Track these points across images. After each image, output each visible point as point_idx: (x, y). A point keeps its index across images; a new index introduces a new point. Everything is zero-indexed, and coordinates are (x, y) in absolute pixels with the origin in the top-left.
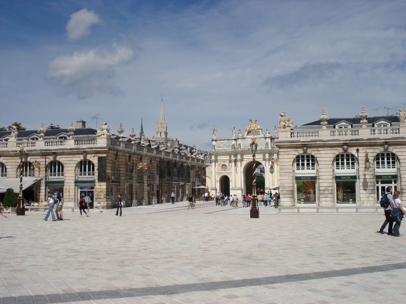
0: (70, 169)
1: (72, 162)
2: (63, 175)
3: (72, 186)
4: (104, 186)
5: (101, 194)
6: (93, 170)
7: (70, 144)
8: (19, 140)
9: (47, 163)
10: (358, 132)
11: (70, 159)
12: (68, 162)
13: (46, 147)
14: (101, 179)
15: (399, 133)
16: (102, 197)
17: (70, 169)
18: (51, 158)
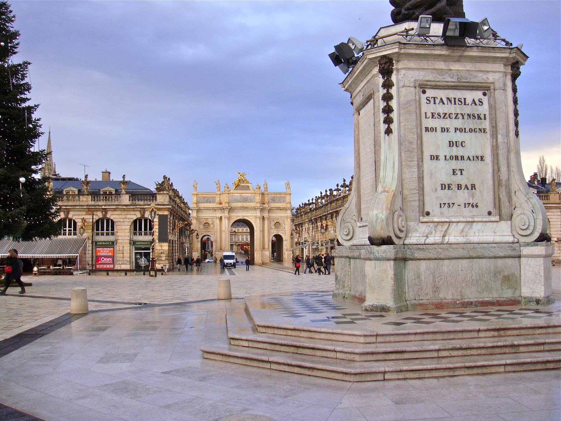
0: (124, 227)
1: (126, 220)
2: (113, 234)
3: (127, 247)
4: (165, 246)
5: (162, 255)
6: (151, 228)
9: (95, 220)
11: (124, 217)
12: (122, 220)
14: (163, 238)
16: (164, 258)
17: (124, 227)
18: (100, 215)
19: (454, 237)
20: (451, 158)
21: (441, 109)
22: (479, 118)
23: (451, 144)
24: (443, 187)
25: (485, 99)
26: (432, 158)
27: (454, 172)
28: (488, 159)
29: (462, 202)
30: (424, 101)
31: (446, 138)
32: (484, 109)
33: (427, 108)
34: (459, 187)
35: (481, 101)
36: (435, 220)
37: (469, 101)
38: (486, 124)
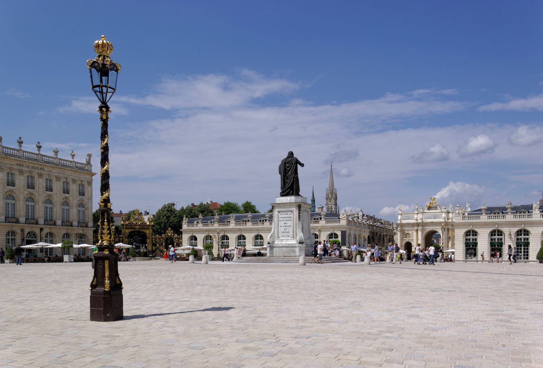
7: (322, 223)
8: (237, 222)
10: (480, 217)
13: (270, 226)
15: (480, 219)
19: (284, 242)
20: (284, 226)
21: (283, 216)
22: (290, 217)
23: (284, 223)
24: (282, 232)
25: (292, 213)
26: (281, 226)
27: (285, 229)
28: (292, 226)
29: (286, 235)
30: (279, 214)
31: (283, 222)
32: (291, 216)
33: (280, 216)
34: (286, 232)
35: (291, 214)
36: (281, 239)
37: (289, 214)
38: (292, 219)
